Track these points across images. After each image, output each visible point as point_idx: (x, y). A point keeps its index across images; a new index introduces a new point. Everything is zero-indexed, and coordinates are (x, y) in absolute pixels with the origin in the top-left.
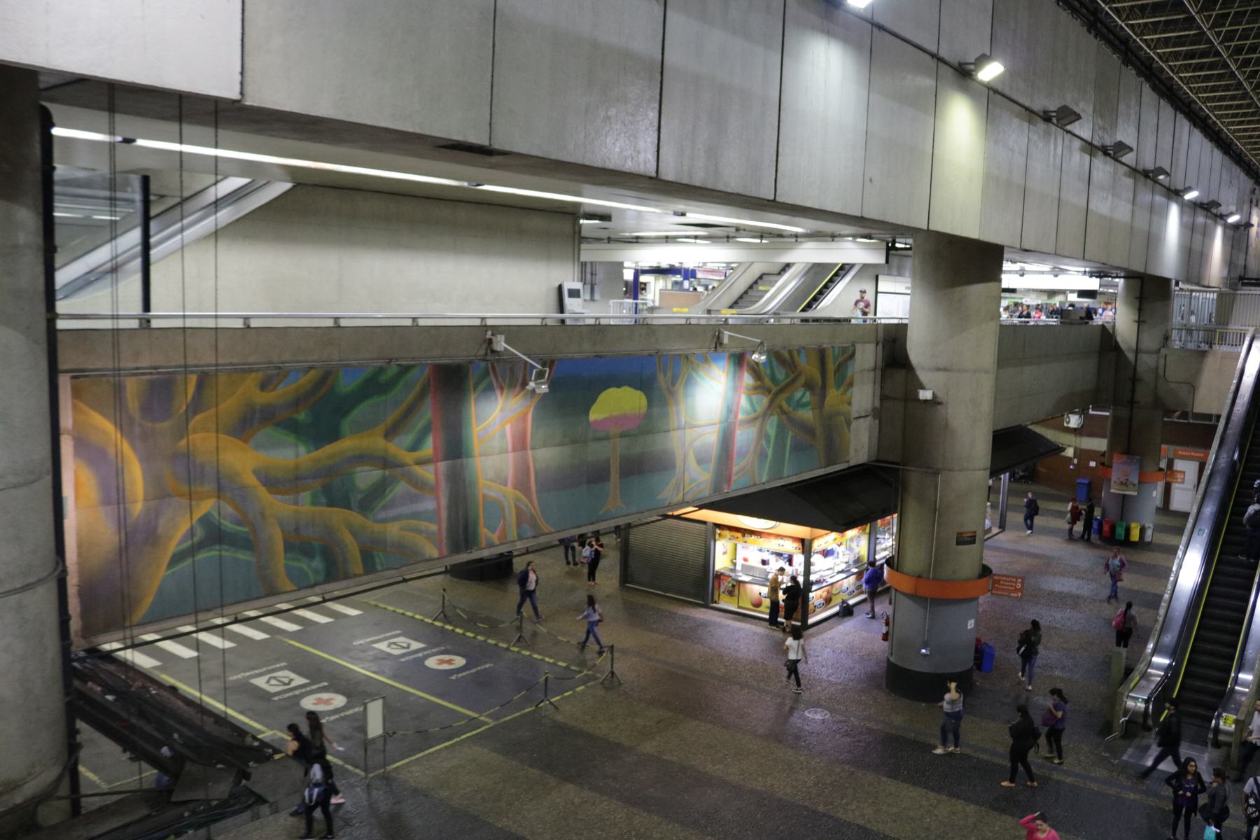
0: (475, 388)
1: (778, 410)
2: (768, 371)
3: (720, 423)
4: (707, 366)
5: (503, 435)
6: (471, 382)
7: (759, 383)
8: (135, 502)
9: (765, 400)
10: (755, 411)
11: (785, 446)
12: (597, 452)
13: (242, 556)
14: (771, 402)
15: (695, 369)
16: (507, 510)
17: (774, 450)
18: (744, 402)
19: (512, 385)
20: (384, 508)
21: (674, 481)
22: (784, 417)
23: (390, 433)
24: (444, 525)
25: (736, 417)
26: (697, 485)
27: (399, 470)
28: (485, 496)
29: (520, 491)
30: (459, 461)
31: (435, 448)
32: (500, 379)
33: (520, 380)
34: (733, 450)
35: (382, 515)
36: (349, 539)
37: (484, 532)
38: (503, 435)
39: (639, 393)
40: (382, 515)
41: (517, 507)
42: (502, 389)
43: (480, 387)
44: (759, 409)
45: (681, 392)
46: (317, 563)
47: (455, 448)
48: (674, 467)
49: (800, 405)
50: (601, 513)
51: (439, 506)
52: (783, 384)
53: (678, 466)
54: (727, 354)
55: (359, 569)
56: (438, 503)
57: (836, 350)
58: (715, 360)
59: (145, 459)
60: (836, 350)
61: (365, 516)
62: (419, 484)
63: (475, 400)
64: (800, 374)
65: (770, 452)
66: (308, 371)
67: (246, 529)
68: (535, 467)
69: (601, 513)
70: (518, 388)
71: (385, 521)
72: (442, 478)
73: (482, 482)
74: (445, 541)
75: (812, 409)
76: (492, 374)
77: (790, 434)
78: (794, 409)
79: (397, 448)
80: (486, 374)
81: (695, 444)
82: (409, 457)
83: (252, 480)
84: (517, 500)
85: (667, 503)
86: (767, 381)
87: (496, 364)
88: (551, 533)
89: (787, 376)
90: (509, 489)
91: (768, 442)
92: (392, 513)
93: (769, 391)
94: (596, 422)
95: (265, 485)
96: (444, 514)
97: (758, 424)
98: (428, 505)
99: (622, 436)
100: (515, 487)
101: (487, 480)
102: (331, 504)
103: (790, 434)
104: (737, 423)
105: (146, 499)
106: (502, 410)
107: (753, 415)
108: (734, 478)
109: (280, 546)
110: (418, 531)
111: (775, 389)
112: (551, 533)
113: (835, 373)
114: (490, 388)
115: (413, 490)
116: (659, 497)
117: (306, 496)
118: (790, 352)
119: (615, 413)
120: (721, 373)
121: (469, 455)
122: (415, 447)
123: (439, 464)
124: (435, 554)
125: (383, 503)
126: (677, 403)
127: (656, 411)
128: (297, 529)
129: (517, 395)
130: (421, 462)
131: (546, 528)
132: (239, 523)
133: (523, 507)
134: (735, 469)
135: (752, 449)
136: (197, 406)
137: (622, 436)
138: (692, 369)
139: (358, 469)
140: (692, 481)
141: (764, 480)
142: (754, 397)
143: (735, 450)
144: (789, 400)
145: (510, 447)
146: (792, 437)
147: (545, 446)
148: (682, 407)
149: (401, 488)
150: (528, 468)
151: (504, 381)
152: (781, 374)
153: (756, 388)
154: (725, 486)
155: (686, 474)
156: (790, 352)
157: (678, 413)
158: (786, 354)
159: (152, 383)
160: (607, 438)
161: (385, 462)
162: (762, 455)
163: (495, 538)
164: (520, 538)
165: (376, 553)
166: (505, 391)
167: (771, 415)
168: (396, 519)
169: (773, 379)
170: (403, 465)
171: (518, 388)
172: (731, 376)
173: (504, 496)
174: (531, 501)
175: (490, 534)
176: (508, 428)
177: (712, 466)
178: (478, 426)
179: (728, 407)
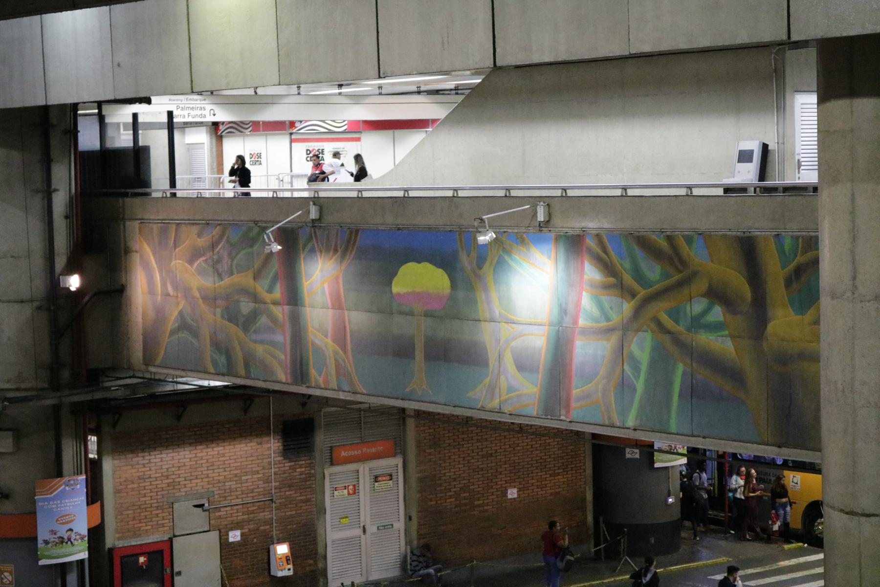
0: (304, 249)
1: (653, 326)
2: (627, 265)
3: (550, 325)
4: (524, 249)
5: (323, 293)
6: (301, 242)
7: (612, 280)
8: (158, 295)
9: (628, 307)
10: (608, 319)
11: (669, 384)
12: (402, 326)
13: (194, 341)
14: (637, 312)
15: (509, 252)
16: (328, 360)
17: (647, 381)
18: (587, 302)
19: (328, 250)
20: (255, 332)
21: (487, 381)
22: (667, 338)
23: (256, 277)
24: (289, 357)
25: (576, 322)
26: (519, 396)
27: (262, 306)
28: (313, 344)
29: (337, 344)
30: (297, 307)
31: (282, 294)
32: (319, 243)
33: (333, 246)
34: (571, 365)
35: (254, 337)
36: (238, 348)
37: (313, 373)
38: (323, 293)
39: (441, 270)
40: (254, 337)
41: (336, 360)
42: (321, 252)
43: (307, 250)
44: (616, 319)
45: (490, 278)
46: (223, 359)
47: (294, 297)
48: (486, 364)
49: (697, 323)
50: (407, 390)
51: (285, 339)
52: (658, 287)
53: (491, 366)
54: (553, 235)
55: (243, 373)
56: (285, 339)
57: (787, 242)
58: (537, 241)
59: (161, 272)
60: (787, 242)
61: (245, 334)
62: (273, 319)
63: (304, 258)
64: (695, 274)
65: (640, 385)
66: (216, 227)
67: (195, 324)
68: (350, 327)
69: (407, 390)
70: (331, 253)
71: (256, 342)
72: (287, 318)
73: (310, 329)
74: (289, 371)
75: (732, 337)
76: (314, 238)
77: (680, 368)
78: (689, 330)
79: (261, 288)
80: (310, 238)
81: (514, 344)
82: (268, 297)
83: (197, 294)
84: (336, 353)
85: (479, 406)
86: (628, 279)
87: (317, 230)
88: (362, 394)
89: (665, 276)
90: (329, 341)
91: (636, 369)
92: (260, 337)
93: (633, 295)
94: (399, 295)
95: (202, 299)
96: (288, 348)
97: (615, 338)
98: (279, 338)
99: (427, 314)
100: (334, 341)
101: (313, 328)
102: (230, 320)
103: (680, 368)
104: (577, 329)
105: (161, 295)
106: (321, 271)
107: (604, 324)
108: (574, 405)
109: (208, 342)
110: (273, 356)
111: (642, 293)
112: (362, 394)
113: (788, 282)
114: (313, 251)
115: (271, 324)
116: (470, 394)
117: (219, 311)
118: (670, 239)
119: (418, 290)
120: (546, 260)
121: (303, 305)
122: (270, 290)
123: (285, 307)
124: (283, 378)
125: (254, 328)
126: (486, 289)
127: (461, 294)
128: (215, 333)
129: (331, 259)
130: (275, 303)
131: (360, 388)
132: (193, 320)
133: (341, 361)
134: (575, 392)
135: (603, 371)
136: (175, 246)
137: (427, 314)
138: (504, 250)
139: (242, 299)
140: (511, 389)
141: (631, 422)
142: (606, 300)
143: (574, 370)
144: (675, 314)
145: (330, 304)
146: (684, 374)
147: (356, 310)
148: (494, 296)
149: (263, 320)
150: (345, 327)
151: (322, 245)
152: (653, 271)
153: (606, 287)
154: (563, 412)
155: (502, 378)
156: (670, 239)
157: (489, 302)
158: (663, 244)
159: (161, 227)
160: (411, 314)
161: (255, 298)
162: (624, 386)
163: (321, 380)
164: (340, 389)
165: (251, 363)
166: (323, 254)
167: (637, 331)
168: (262, 342)
169: (638, 275)
170: (265, 303)
171: (331, 253)
172: (561, 265)
173: (326, 346)
174: (347, 358)
175: (318, 377)
176: (326, 286)
177: (540, 377)
178: (306, 282)
179: (560, 306)
